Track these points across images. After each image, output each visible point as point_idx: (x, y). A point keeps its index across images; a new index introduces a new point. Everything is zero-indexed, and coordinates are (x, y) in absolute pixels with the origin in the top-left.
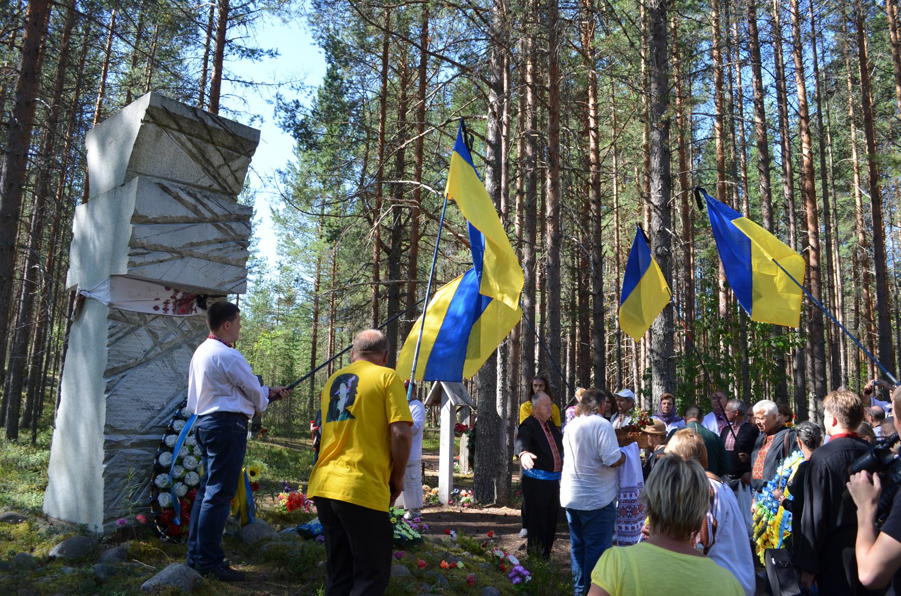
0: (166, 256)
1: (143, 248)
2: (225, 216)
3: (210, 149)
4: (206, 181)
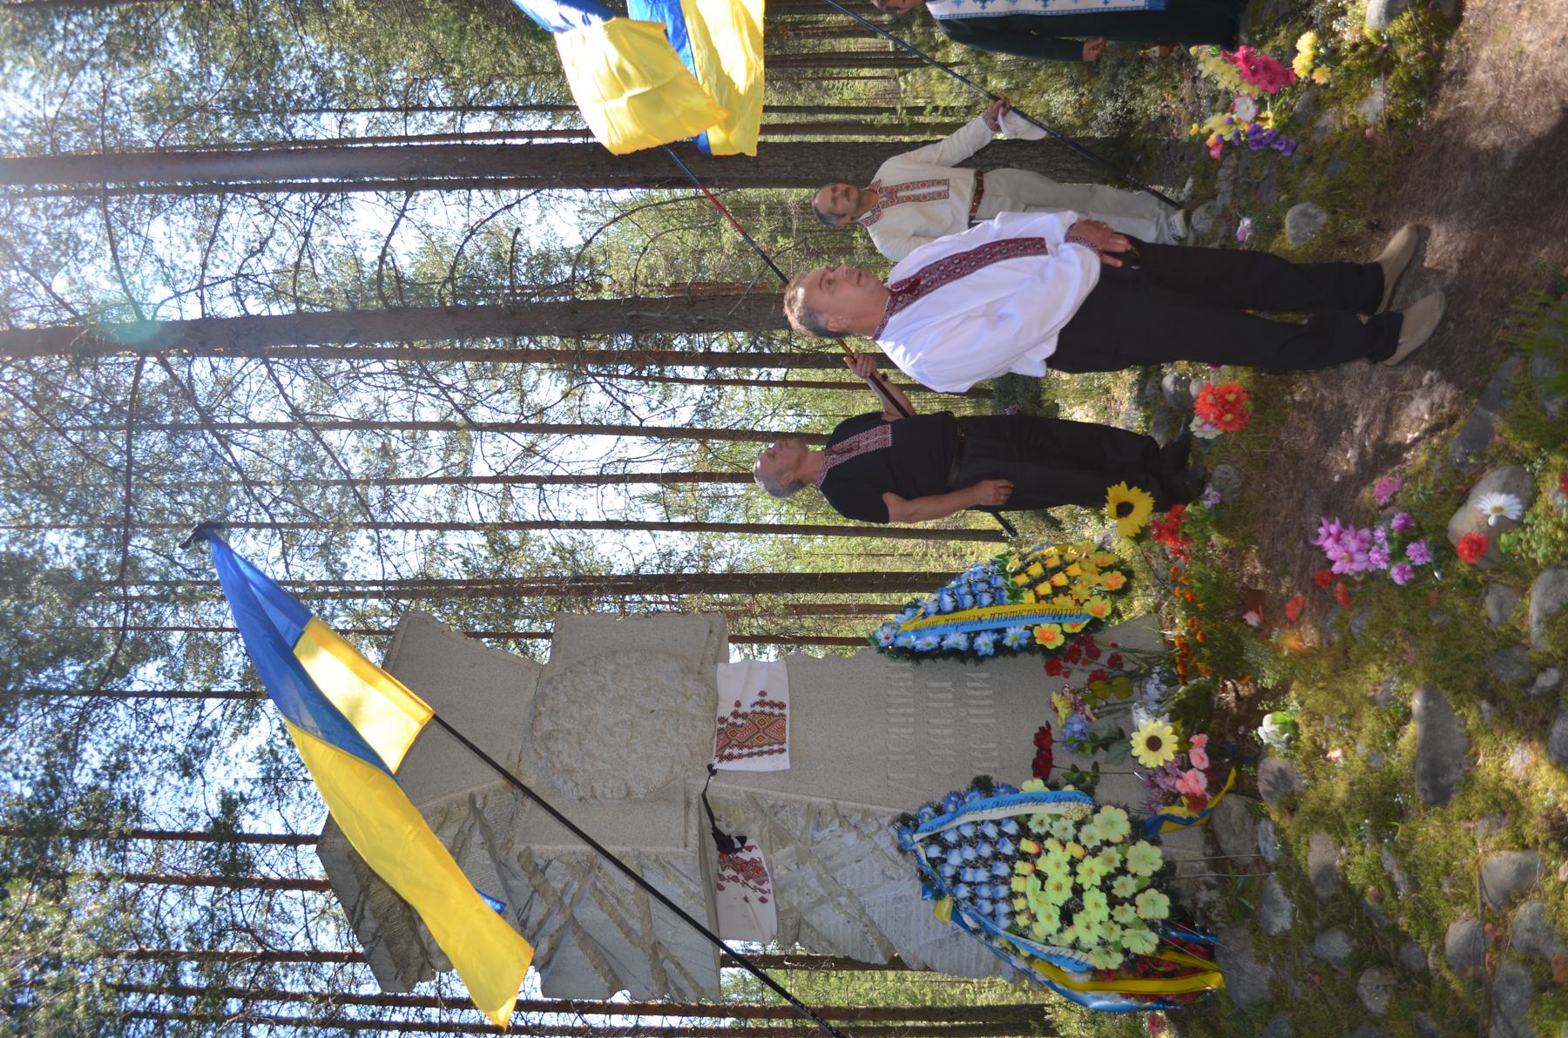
0: (669, 966)
1: (666, 984)
2: (544, 895)
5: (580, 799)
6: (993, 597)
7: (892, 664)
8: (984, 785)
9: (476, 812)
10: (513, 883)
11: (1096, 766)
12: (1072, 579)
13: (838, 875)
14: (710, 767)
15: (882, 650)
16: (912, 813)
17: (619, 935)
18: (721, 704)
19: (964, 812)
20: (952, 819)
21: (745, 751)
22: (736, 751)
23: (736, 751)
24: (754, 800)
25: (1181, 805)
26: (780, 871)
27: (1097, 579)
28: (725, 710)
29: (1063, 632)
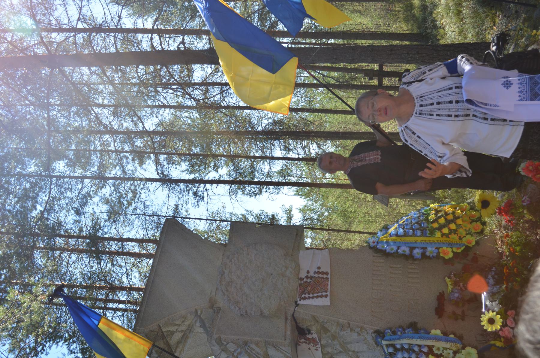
3: (173, 341)
5: (241, 315)
6: (422, 233)
7: (376, 255)
8: (414, 327)
10: (213, 348)
11: (463, 312)
12: (459, 226)
13: (349, 346)
14: (296, 302)
15: (371, 248)
16: (382, 331)
18: (301, 271)
19: (405, 338)
20: (400, 338)
21: (311, 295)
22: (307, 296)
23: (307, 296)
25: (501, 341)
27: (469, 226)
28: (303, 274)
29: (453, 251)
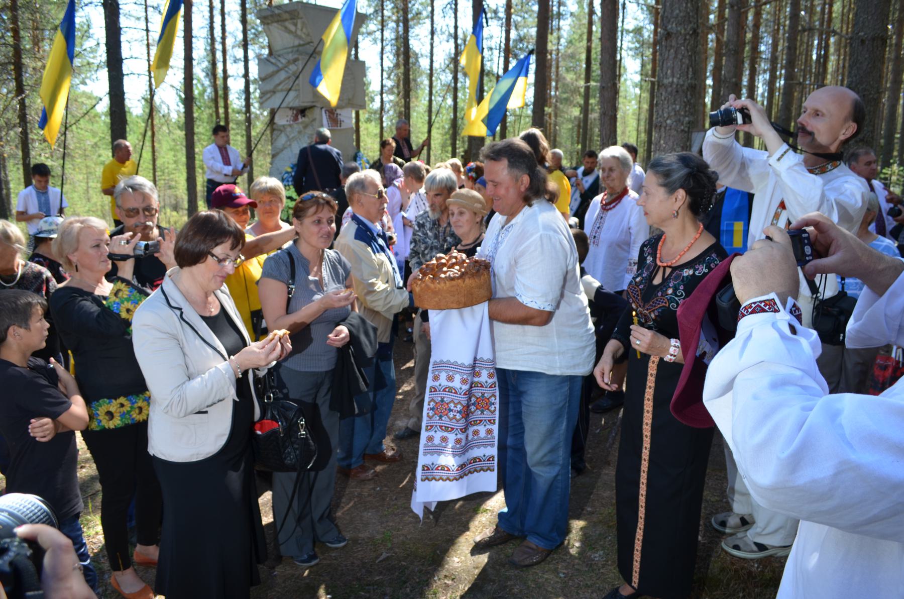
0: (269, 95)
3: (287, 24)
4: (297, 42)
9: (309, 43)
17: (277, 82)
24: (314, 120)
26: (295, 126)
28: (338, 111)
